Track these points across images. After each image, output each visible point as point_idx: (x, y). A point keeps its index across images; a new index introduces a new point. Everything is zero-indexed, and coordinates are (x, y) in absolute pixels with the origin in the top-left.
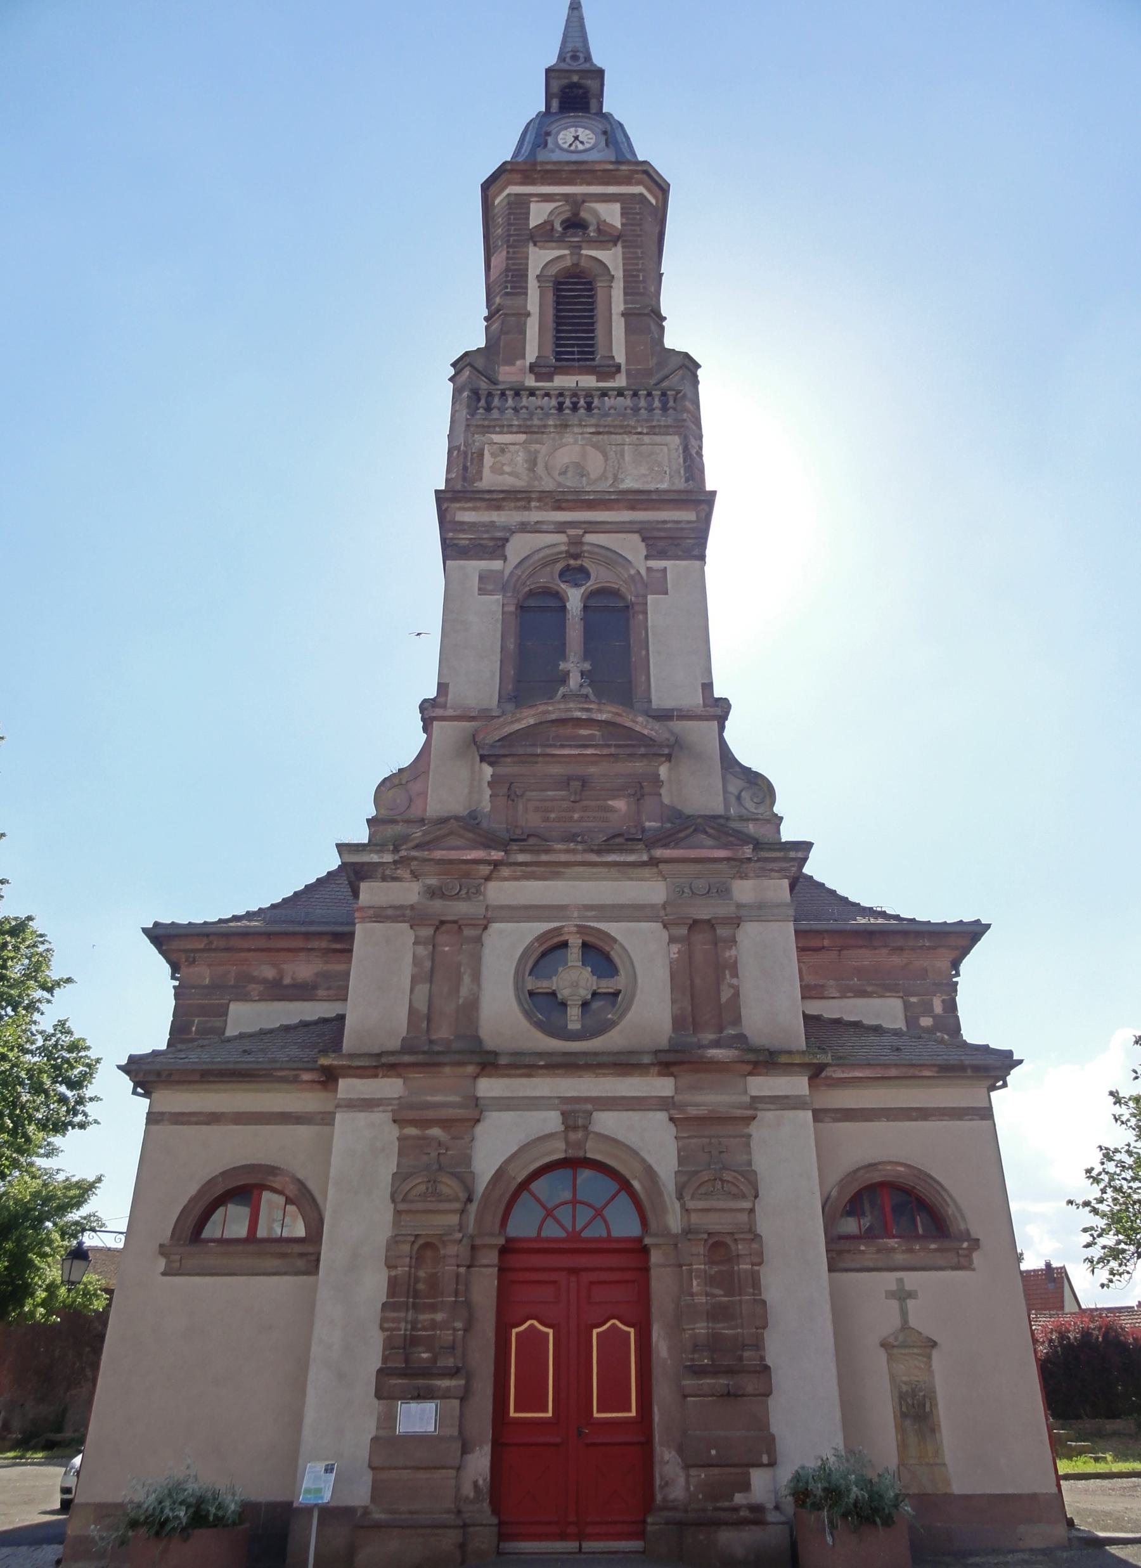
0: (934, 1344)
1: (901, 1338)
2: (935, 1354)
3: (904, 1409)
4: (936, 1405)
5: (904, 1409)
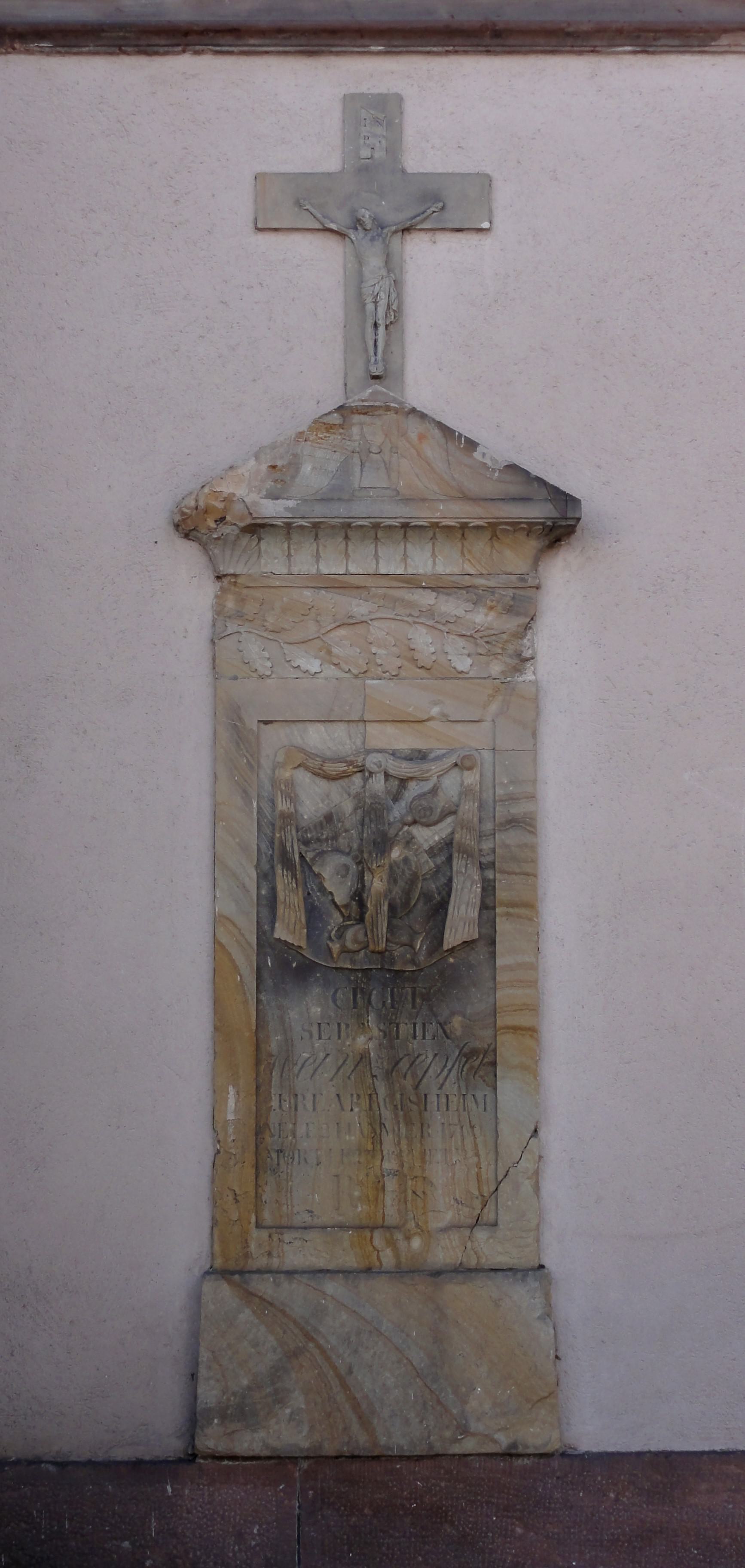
0: (558, 524)
1: (314, 473)
2: (564, 580)
3: (289, 929)
4: (528, 907)
5: (289, 929)
